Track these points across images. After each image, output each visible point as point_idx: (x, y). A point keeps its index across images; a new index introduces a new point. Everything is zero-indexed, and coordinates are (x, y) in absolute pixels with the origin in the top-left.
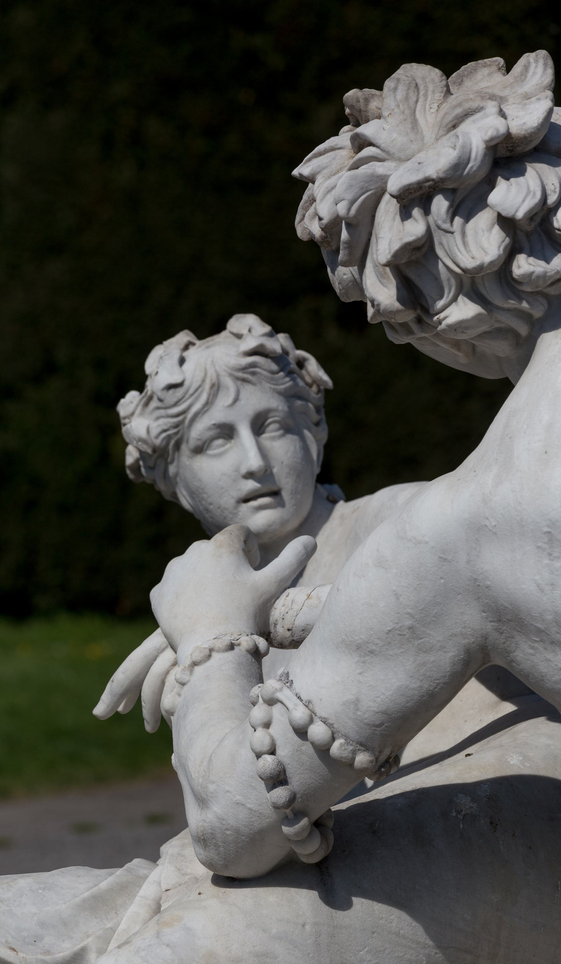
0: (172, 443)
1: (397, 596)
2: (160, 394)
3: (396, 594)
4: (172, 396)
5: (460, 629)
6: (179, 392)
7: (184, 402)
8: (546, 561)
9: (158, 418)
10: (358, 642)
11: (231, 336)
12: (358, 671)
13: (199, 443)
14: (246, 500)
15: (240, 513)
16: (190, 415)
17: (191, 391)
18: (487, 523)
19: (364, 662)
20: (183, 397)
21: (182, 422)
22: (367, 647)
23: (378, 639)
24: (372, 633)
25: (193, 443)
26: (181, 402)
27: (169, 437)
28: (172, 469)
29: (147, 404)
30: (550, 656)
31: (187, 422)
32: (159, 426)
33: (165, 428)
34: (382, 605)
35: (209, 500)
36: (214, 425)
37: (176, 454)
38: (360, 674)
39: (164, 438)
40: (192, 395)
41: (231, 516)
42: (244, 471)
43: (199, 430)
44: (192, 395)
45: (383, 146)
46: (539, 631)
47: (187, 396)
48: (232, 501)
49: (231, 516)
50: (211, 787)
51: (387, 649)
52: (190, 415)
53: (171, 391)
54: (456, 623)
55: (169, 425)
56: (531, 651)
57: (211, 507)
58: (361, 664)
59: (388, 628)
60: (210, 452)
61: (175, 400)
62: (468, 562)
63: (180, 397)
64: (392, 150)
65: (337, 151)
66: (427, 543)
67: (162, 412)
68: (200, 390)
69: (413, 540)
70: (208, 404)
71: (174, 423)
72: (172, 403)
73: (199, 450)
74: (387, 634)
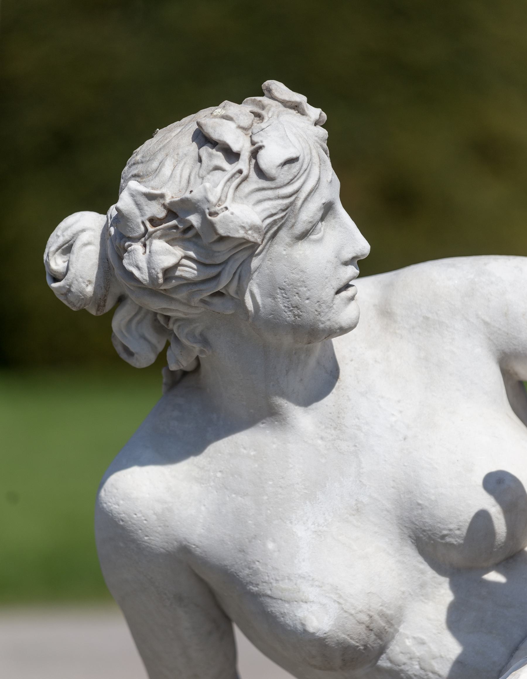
0: (275, 228)
6: (295, 168)
7: (298, 179)
9: (260, 201)
11: (280, 104)
13: (309, 226)
14: (338, 292)
15: (335, 306)
16: (303, 195)
17: (305, 167)
20: (299, 173)
21: (292, 203)
25: (299, 228)
26: (296, 179)
27: (275, 222)
28: (255, 263)
31: (299, 203)
32: (264, 210)
33: (274, 211)
35: (308, 294)
36: (324, 204)
37: (269, 243)
39: (268, 224)
40: (305, 170)
41: (327, 310)
42: (348, 255)
43: (310, 211)
44: (305, 170)
47: (302, 172)
48: (333, 292)
49: (327, 310)
52: (303, 195)
53: (286, 167)
55: (279, 208)
57: (307, 301)
60: (313, 237)
61: (291, 178)
63: (296, 174)
67: (270, 193)
68: (310, 165)
71: (286, 204)
72: (286, 182)
73: (303, 236)
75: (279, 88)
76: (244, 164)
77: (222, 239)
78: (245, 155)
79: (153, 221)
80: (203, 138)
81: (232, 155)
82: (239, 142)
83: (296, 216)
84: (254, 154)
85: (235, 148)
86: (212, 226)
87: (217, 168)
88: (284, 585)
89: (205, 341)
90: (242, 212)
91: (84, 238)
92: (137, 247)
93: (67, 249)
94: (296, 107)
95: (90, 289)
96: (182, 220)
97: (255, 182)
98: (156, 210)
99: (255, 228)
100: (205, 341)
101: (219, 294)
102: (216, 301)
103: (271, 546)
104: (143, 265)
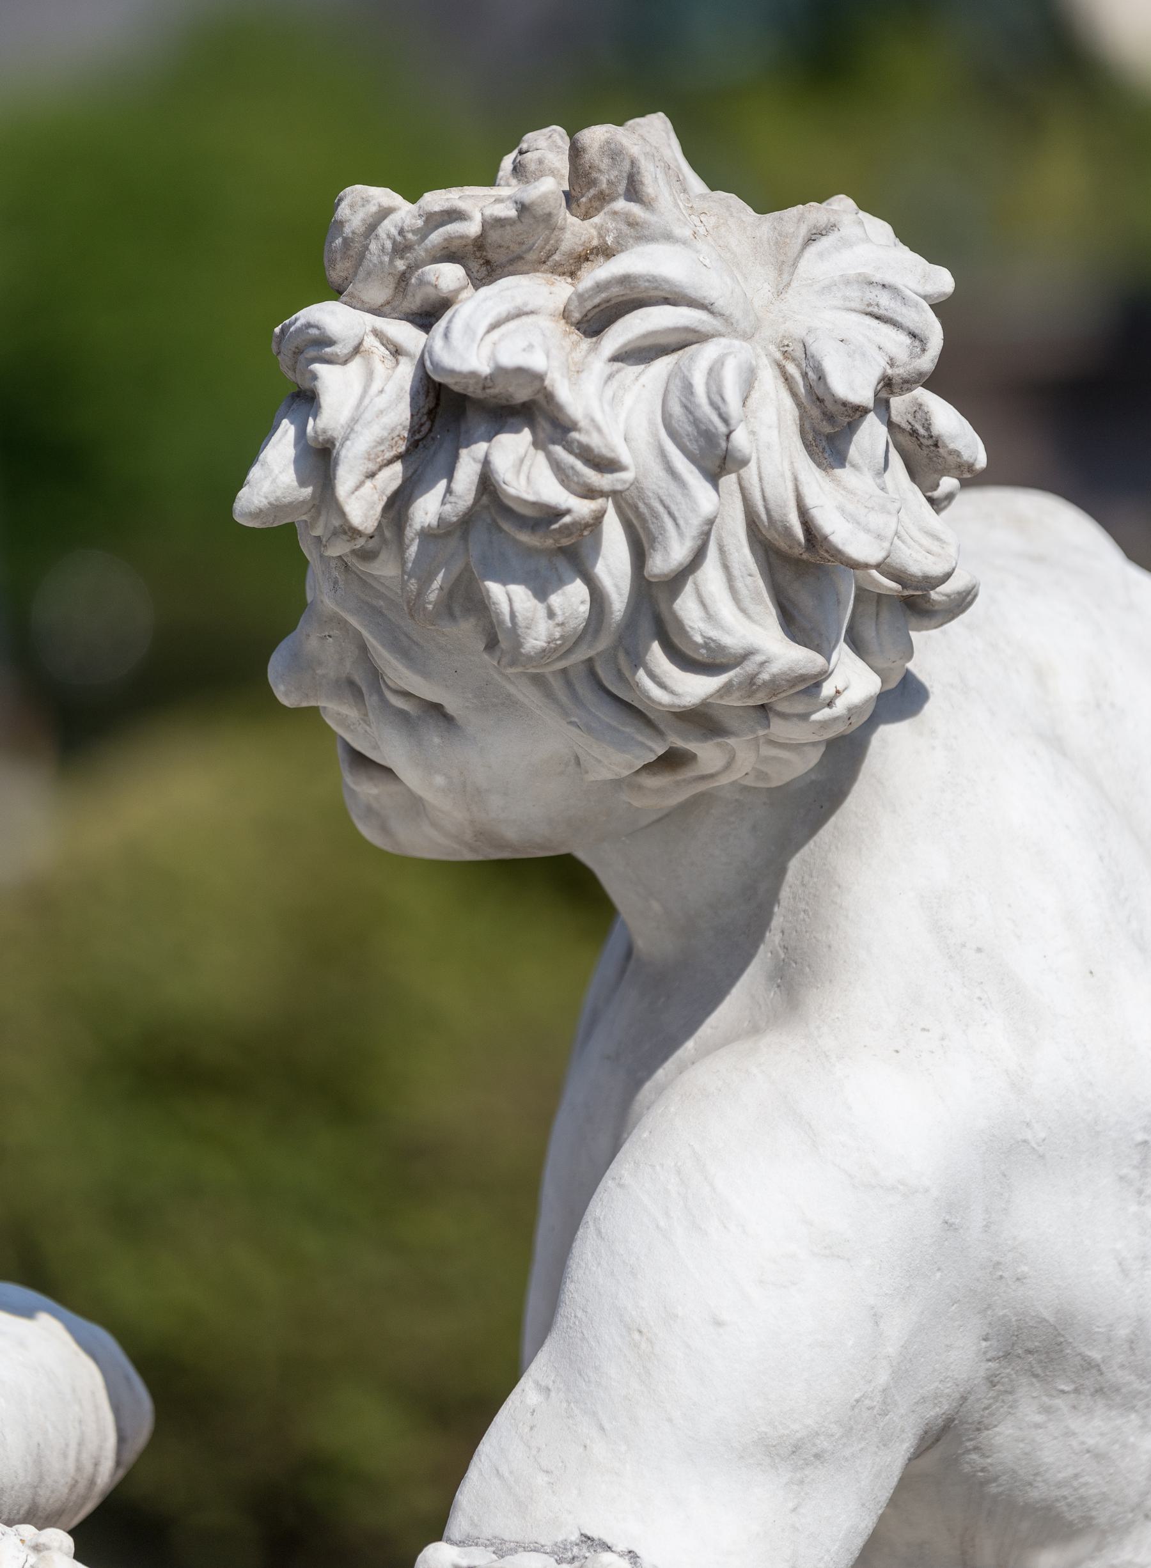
3: (875, 1315)
5: (936, 1384)
8: (1133, 1208)
10: (798, 1435)
12: (791, 1505)
18: (1029, 1136)
19: (801, 1482)
22: (814, 1445)
23: (836, 1423)
24: (828, 1410)
30: (1075, 1423)
34: (851, 1343)
38: (794, 1510)
45: (720, 304)
46: (1090, 1366)
51: (844, 1445)
54: (935, 1370)
56: (1039, 1418)
58: (795, 1487)
59: (857, 1396)
62: (987, 1226)
64: (737, 314)
65: (524, 319)
66: (927, 1191)
69: (901, 1187)
74: (853, 1408)
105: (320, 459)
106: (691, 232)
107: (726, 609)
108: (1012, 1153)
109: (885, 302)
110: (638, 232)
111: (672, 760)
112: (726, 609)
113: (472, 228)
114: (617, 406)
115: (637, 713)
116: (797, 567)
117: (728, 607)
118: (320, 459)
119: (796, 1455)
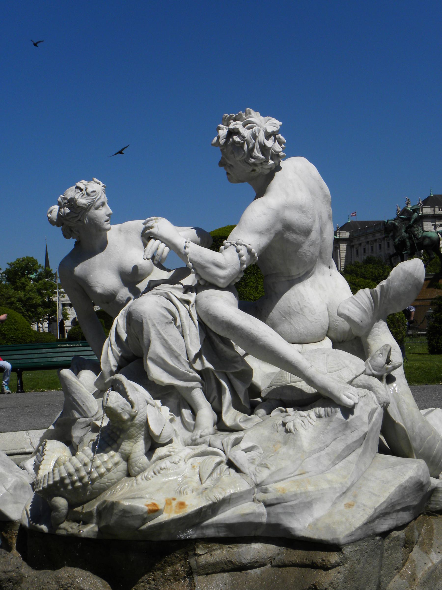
1: (269, 221)
2: (90, 193)
4: (93, 194)
14: (105, 222)
29: (82, 196)
42: (108, 213)
50: (229, 265)
70: (101, 197)
73: (97, 208)
75: (96, 180)
76: (84, 192)
77: (79, 207)
78: (84, 190)
79: (65, 203)
80: (77, 187)
81: (81, 190)
82: (82, 187)
83: (95, 203)
84: (86, 190)
85: (82, 188)
86: (76, 203)
87: (79, 193)
88: (93, 284)
89: (78, 232)
90: (82, 201)
91: (54, 210)
92: (62, 209)
93: (51, 212)
94: (99, 184)
95: (55, 220)
96: (71, 203)
97: (86, 196)
98: (66, 201)
99: (85, 205)
100: (78, 232)
101: (79, 220)
102: (79, 222)
103: (91, 276)
104: (63, 213)
105: (218, 138)
106: (255, 117)
107: (256, 153)
108: (285, 207)
109: (275, 125)
110: (251, 117)
111: (254, 170)
112: (256, 153)
113: (234, 117)
114: (246, 133)
115: (248, 164)
116: (264, 149)
117: (257, 153)
118: (218, 138)
119: (261, 233)
